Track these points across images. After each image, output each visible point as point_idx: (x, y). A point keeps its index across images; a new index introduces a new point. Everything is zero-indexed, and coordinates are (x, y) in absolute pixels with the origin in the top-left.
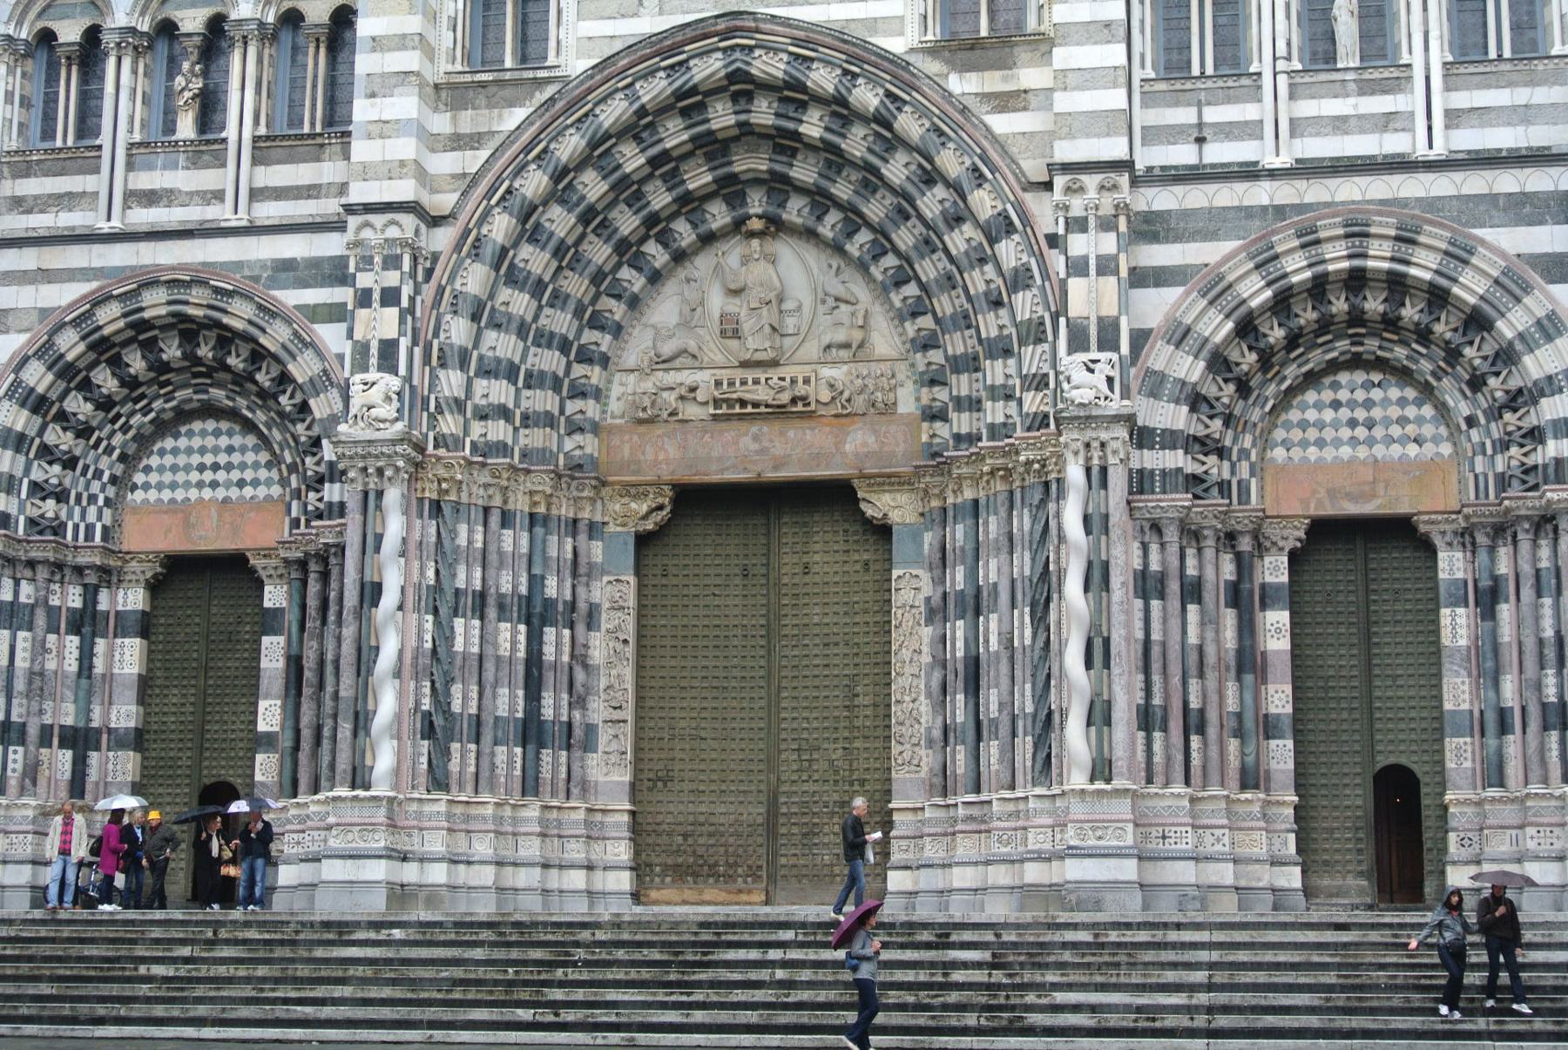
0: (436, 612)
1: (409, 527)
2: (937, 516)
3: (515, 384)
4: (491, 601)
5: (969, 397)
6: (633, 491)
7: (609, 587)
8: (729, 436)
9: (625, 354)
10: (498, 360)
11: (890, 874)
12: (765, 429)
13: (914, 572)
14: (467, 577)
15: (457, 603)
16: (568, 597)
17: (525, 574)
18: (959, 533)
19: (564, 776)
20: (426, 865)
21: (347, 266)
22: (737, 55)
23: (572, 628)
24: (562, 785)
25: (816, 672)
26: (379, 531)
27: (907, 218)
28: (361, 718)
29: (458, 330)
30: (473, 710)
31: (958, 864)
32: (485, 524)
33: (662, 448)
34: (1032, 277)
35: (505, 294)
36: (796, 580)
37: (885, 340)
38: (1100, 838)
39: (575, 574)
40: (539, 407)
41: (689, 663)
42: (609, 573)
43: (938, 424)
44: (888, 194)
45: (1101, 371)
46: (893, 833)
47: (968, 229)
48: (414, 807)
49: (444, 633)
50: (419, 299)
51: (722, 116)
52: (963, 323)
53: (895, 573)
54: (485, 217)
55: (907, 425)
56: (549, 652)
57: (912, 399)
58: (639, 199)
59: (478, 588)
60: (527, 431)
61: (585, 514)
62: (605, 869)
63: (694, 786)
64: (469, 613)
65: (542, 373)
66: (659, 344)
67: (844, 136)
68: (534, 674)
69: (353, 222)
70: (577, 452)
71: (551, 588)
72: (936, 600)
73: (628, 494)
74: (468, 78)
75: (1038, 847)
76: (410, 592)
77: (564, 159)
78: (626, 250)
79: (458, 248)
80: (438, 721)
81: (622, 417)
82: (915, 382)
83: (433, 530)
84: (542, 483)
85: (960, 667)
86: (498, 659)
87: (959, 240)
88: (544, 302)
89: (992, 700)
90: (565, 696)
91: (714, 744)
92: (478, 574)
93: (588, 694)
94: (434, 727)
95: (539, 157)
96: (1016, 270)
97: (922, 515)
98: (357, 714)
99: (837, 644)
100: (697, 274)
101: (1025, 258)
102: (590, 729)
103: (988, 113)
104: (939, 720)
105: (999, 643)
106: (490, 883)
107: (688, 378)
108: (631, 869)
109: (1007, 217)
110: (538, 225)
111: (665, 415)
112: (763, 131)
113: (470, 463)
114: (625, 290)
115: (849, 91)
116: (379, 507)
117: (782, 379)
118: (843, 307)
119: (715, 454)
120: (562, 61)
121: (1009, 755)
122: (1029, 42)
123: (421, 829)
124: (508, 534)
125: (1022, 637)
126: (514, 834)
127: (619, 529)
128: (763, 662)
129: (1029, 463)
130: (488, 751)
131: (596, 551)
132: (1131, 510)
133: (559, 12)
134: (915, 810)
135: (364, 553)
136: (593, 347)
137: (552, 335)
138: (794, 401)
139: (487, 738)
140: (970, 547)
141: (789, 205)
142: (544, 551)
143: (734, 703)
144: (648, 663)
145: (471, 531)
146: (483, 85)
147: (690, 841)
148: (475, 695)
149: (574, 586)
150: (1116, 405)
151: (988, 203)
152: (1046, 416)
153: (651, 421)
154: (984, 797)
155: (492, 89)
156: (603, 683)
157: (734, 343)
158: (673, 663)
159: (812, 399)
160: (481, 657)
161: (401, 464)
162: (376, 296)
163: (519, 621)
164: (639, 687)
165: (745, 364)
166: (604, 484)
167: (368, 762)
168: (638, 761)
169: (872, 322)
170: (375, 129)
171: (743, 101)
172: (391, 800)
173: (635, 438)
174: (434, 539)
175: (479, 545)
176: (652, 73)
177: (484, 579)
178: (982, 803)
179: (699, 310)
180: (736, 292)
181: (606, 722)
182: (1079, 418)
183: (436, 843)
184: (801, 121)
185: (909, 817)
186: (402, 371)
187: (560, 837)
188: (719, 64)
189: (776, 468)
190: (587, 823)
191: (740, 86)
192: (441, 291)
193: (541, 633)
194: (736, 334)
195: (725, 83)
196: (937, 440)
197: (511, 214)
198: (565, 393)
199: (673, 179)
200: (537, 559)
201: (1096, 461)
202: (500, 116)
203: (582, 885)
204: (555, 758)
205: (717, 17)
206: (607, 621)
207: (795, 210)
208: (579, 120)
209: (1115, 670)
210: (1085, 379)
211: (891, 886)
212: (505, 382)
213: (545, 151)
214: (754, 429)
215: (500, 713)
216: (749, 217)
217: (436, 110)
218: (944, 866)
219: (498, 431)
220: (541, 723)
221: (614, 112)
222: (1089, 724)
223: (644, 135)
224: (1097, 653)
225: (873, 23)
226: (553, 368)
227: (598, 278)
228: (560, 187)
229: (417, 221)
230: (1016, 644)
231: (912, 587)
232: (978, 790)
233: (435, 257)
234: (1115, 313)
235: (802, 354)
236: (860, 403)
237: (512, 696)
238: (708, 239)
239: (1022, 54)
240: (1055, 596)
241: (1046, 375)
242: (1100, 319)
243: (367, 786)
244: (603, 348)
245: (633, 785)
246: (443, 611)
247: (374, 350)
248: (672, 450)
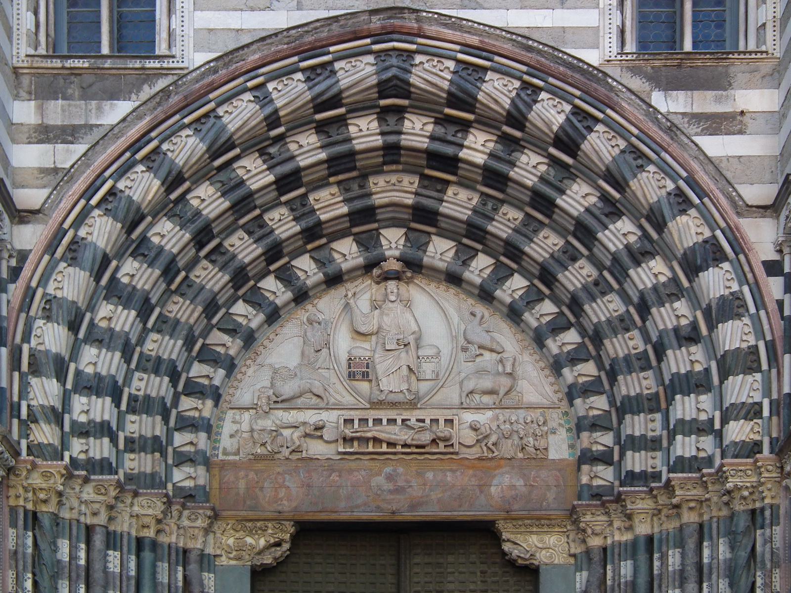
81: (237, 453)
88: (150, 324)
117: (423, 421)
165: (377, 405)
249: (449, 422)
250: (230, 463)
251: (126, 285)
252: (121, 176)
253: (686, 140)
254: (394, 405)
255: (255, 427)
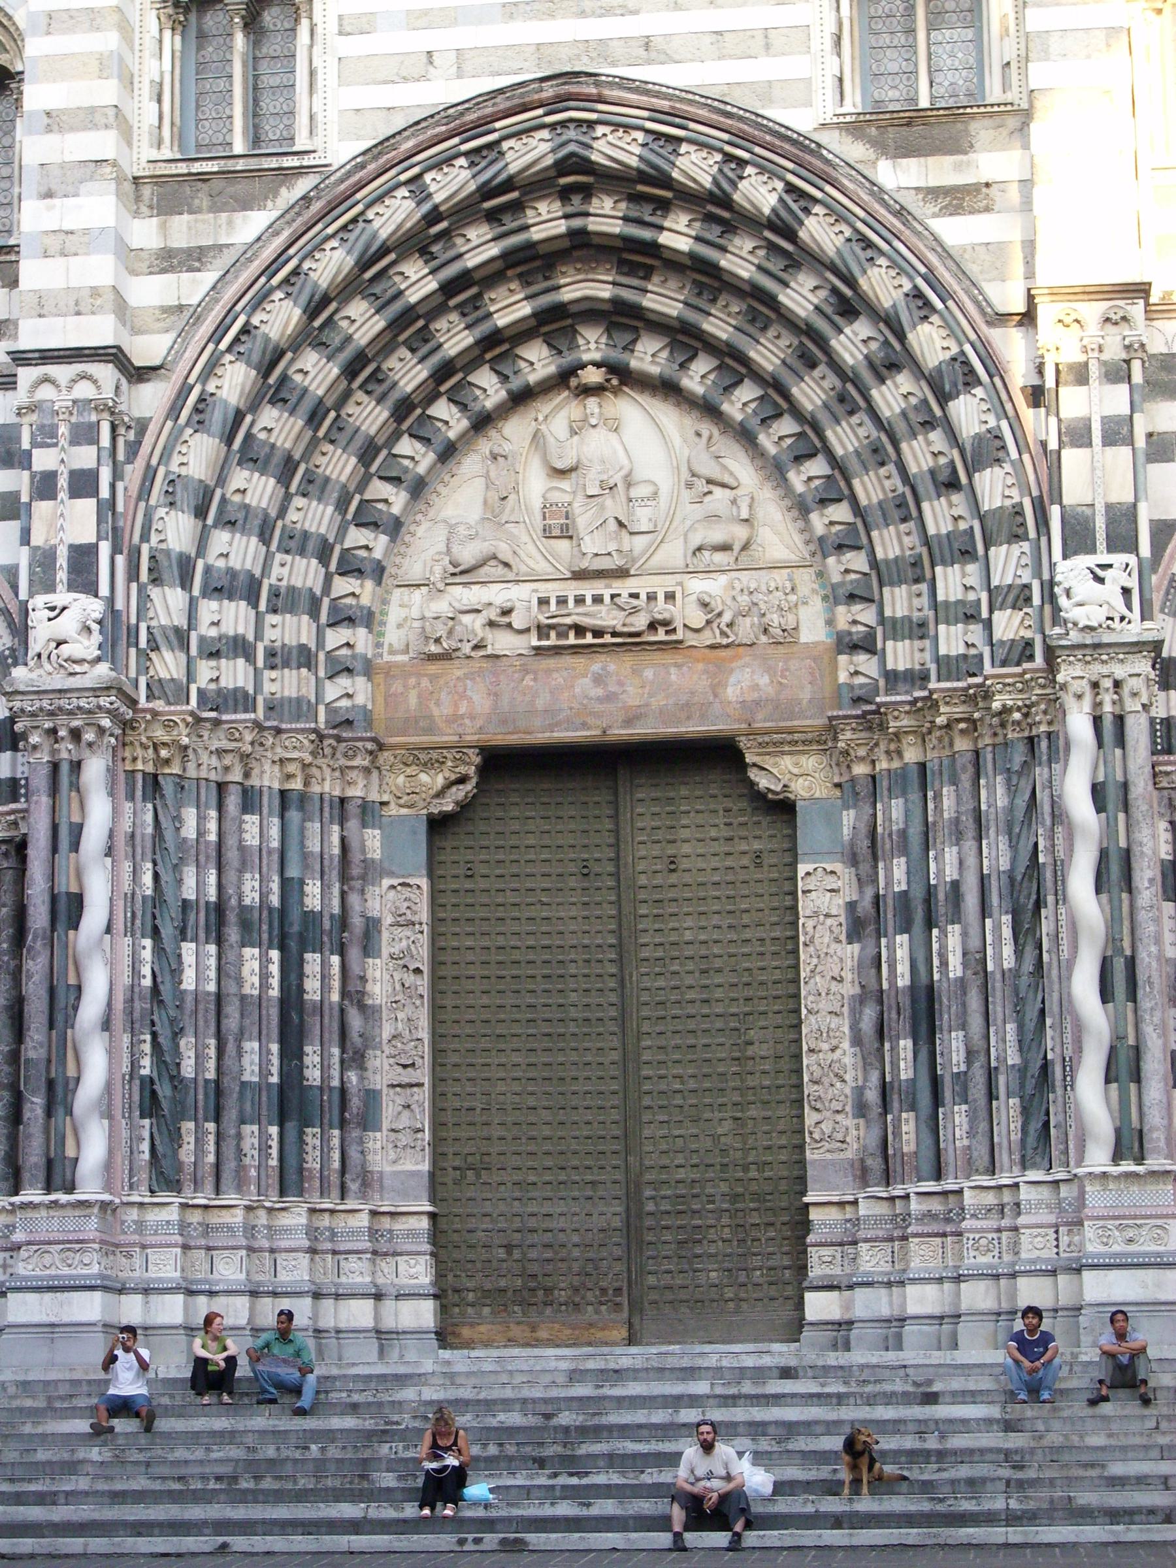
0: (156, 933)
1: (116, 812)
2: (864, 789)
3: (255, 606)
4: (232, 917)
5: (909, 619)
6: (423, 756)
7: (392, 893)
8: (558, 679)
9: (406, 562)
10: (232, 573)
11: (808, 1296)
12: (612, 667)
13: (829, 868)
14: (196, 884)
15: (184, 921)
16: (336, 910)
17: (276, 878)
18: (895, 812)
19: (336, 1165)
20: (153, 1298)
21: (18, 440)
22: (571, 133)
23: (342, 954)
24: (335, 1179)
25: (691, 1010)
26: (76, 819)
27: (812, 365)
28: (59, 1090)
29: (177, 530)
30: (211, 1075)
31: (914, 1281)
32: (220, 808)
33: (463, 696)
34: (1004, 447)
35: (240, 477)
36: (658, 881)
37: (779, 537)
38: (1130, 1241)
39: (344, 878)
40: (291, 640)
41: (510, 1000)
42: (391, 874)
43: (861, 658)
44: (784, 332)
45: (1114, 580)
46: (811, 1239)
47: (904, 382)
48: (133, 1214)
49: (168, 964)
50: (120, 486)
51: (546, 221)
52: (896, 514)
53: (802, 869)
54: (210, 370)
55: (815, 660)
56: (312, 986)
57: (821, 623)
58: (426, 341)
59: (213, 899)
60: (274, 674)
61: (356, 792)
62: (398, 1297)
63: (517, 1177)
64: (202, 935)
65: (292, 590)
66: (455, 549)
67: (724, 250)
68: (292, 1020)
69: (26, 375)
70: (344, 703)
71: (313, 896)
72: (866, 904)
73: (416, 761)
74: (182, 168)
75: (1037, 1253)
76: (121, 903)
77: (324, 284)
78: (407, 412)
79: (174, 411)
80: (164, 1091)
82: (825, 598)
83: (149, 817)
84: (298, 748)
85: (905, 1001)
86: (243, 998)
87: (894, 396)
89: (954, 1049)
90: (336, 1051)
91: (546, 1115)
92: (212, 879)
93: (366, 1047)
94: (157, 1100)
95: (286, 281)
96: (978, 437)
97: (838, 785)
98: (51, 1084)
99: (719, 971)
100: (507, 448)
101: (992, 423)
102: (371, 1097)
103: (935, 216)
104: (874, 1077)
105: (965, 965)
106: (243, 1322)
107: (498, 595)
108: (436, 1297)
109: (966, 363)
110: (284, 379)
111: (467, 648)
112: (605, 241)
113: (199, 720)
114: (406, 470)
115: (734, 185)
116: (76, 786)
117: (635, 596)
118: (718, 492)
119: (540, 704)
120: (317, 143)
121: (983, 1126)
122: (991, 115)
123: (144, 1247)
124: (251, 821)
125: (999, 957)
126: (272, 1251)
127: (404, 811)
128: (613, 998)
129: (1006, 710)
130: (233, 1132)
131: (373, 842)
132: (1155, 775)
133: (312, 73)
134: (841, 1204)
135: (55, 849)
136: (363, 553)
137: (306, 535)
138: (653, 626)
139: (231, 1115)
140: (915, 831)
141: (639, 347)
142: (302, 844)
143: (574, 1057)
144: (449, 1002)
145: (201, 819)
146: (203, 178)
147: (517, 1254)
148: (212, 1052)
149: (343, 894)
150: (1135, 630)
151: (939, 343)
152: (1029, 644)
153: (446, 656)
154: (949, 1184)
155: (217, 184)
156: (387, 1031)
157: (563, 546)
158: (485, 1000)
159: (678, 624)
160: (219, 997)
161: (106, 723)
162: (63, 482)
163: (270, 947)
164: (437, 1036)
166: (381, 747)
167: (70, 1152)
168: (437, 1142)
169: (760, 514)
170: (53, 243)
171: (576, 199)
172: (104, 1205)
173: (425, 682)
174: (150, 830)
175: (213, 837)
176: (449, 161)
177: (220, 886)
178: (945, 1193)
179: (512, 497)
180: (562, 473)
181: (393, 1086)
182: (1085, 646)
183: (165, 1266)
184: (661, 228)
185: (834, 1214)
186: (104, 590)
187: (334, 1252)
188: (545, 147)
189: (628, 722)
190: (373, 1233)
191: (575, 177)
192: (149, 475)
193: (301, 962)
194: (567, 533)
195: (553, 173)
196: (861, 680)
197: (248, 364)
198: (323, 618)
199: (473, 311)
200: (293, 856)
201: (1108, 708)
202: (230, 223)
203: (367, 1321)
204: (325, 1140)
205: (543, 80)
206: (390, 941)
207: (649, 355)
208: (344, 228)
209: (1145, 1004)
210: (1091, 592)
211: (811, 1314)
212: (243, 604)
213: (296, 272)
214: (596, 667)
215: (246, 1077)
216: (583, 366)
217: (137, 214)
218: (889, 1284)
219: (235, 674)
220: (304, 1090)
221: (395, 215)
222: (1108, 1081)
223: (435, 249)
224: (1119, 979)
225: (767, 89)
226: (309, 584)
227: (368, 453)
228: (317, 323)
229: (117, 374)
230: (990, 967)
231: (825, 892)
232: (938, 1176)
233: (142, 426)
234: (1130, 499)
235: (657, 561)
236: (746, 629)
237: (264, 1053)
238: (522, 398)
239: (981, 131)
240: (1050, 899)
241: (1027, 587)
242: (1109, 507)
243: (70, 1188)
244: (377, 554)
245: (432, 1175)
246: (167, 931)
247: (62, 560)
248: (478, 699)
249: (670, 597)
250: (396, 665)
251: (265, 442)
252: (254, 309)
253: (920, 228)
254: (600, 574)
255: (427, 614)
